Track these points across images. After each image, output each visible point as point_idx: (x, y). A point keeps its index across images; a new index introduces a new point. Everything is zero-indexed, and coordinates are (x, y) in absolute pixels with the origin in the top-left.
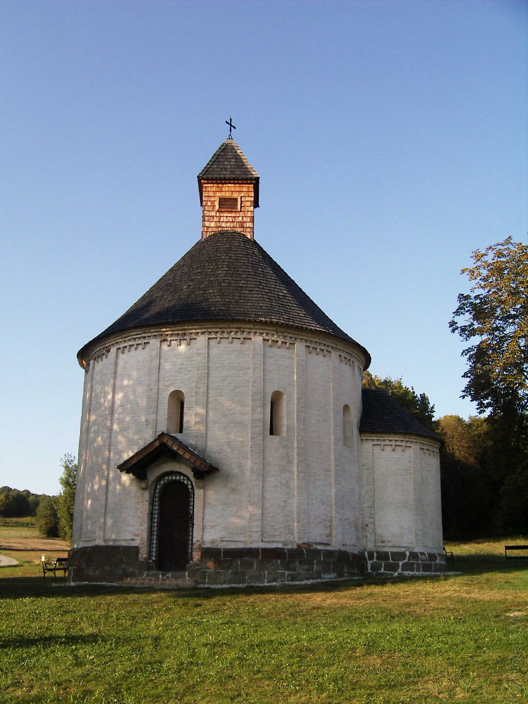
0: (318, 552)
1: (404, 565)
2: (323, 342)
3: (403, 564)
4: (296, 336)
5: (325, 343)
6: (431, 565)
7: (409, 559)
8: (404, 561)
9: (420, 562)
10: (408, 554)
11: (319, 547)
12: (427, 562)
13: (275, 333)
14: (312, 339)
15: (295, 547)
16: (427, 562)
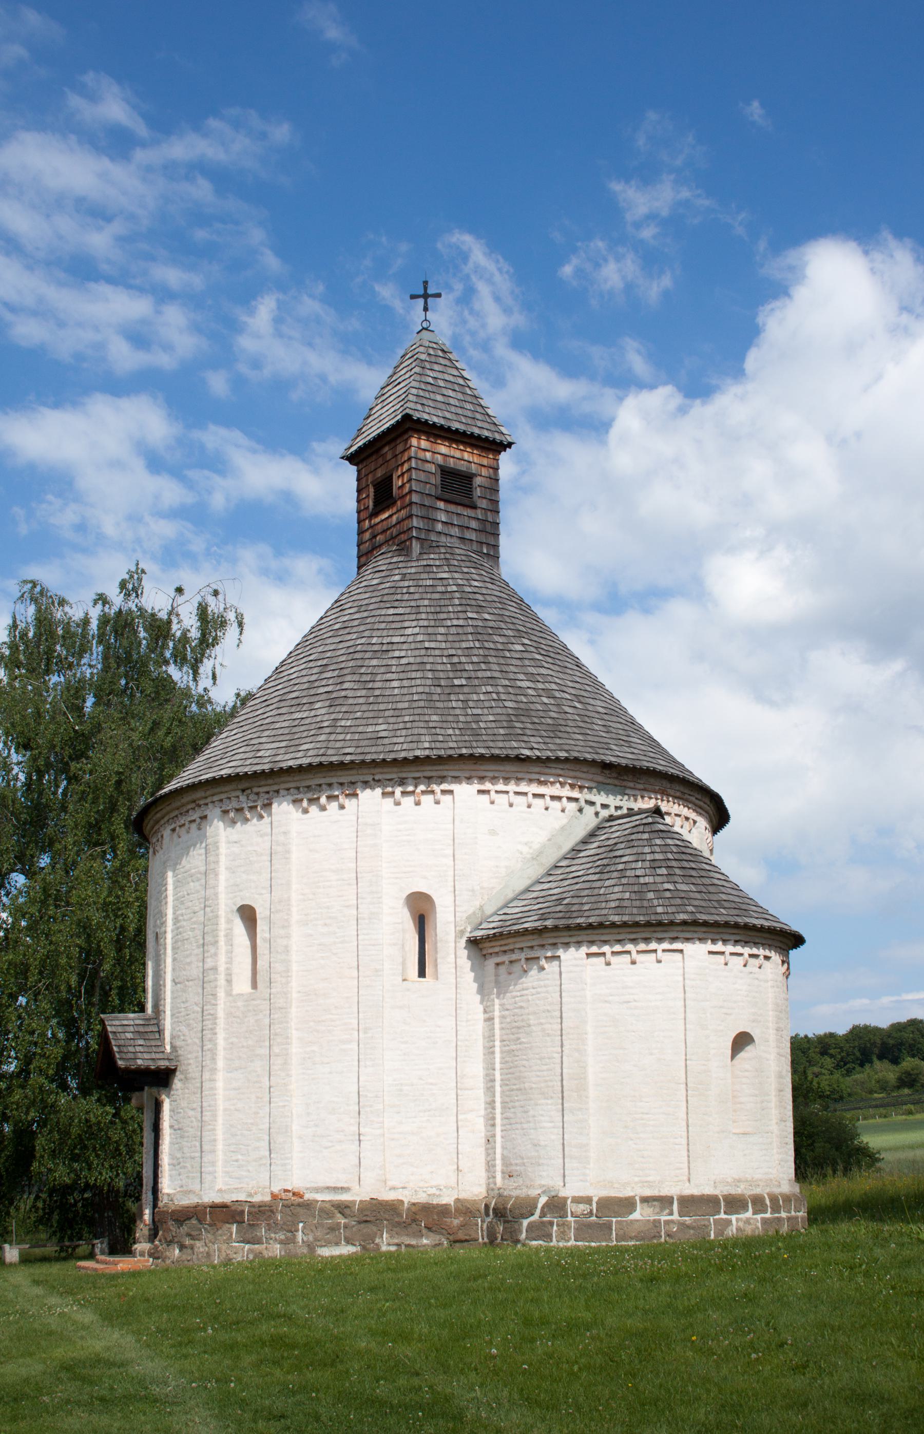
0: (308, 1206)
1: (530, 1227)
2: (334, 780)
3: (529, 1224)
4: (276, 787)
5: (341, 781)
6: (609, 1226)
7: (543, 1214)
8: (532, 1219)
9: (570, 1218)
10: (543, 1200)
11: (319, 1197)
12: (594, 1218)
13: (239, 793)
14: (328, 780)
15: (268, 1198)
16: (594, 1218)
